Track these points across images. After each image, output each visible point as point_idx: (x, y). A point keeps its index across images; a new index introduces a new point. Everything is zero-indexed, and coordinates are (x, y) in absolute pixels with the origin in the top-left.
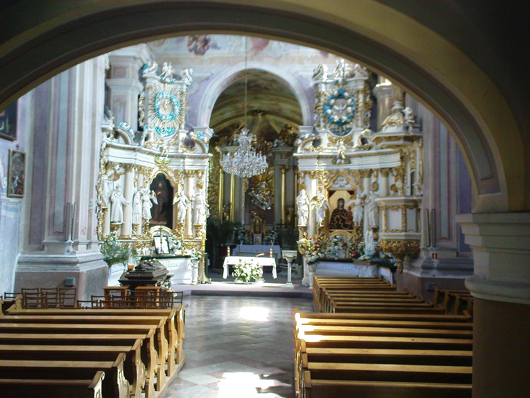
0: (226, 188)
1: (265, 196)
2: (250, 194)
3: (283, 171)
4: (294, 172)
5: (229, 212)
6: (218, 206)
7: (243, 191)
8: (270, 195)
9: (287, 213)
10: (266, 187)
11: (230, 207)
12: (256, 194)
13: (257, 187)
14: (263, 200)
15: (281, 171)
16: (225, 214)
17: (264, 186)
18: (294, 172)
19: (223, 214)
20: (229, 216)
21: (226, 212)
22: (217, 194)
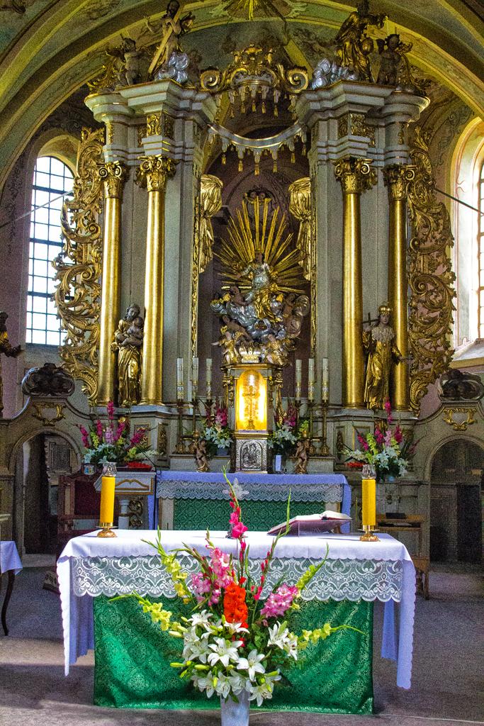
0: (127, 257)
1: (267, 312)
2: (216, 305)
3: (350, 183)
4: (390, 192)
5: (140, 347)
6: (98, 321)
7: (193, 266)
8: (282, 310)
9: (366, 350)
10: (271, 280)
11: (141, 326)
12: (237, 305)
13: (237, 283)
14: (261, 326)
15: (344, 186)
16: (122, 353)
17: (262, 279)
18: (390, 192)
19: (116, 352)
20: (140, 363)
21: (127, 345)
22: (93, 281)
